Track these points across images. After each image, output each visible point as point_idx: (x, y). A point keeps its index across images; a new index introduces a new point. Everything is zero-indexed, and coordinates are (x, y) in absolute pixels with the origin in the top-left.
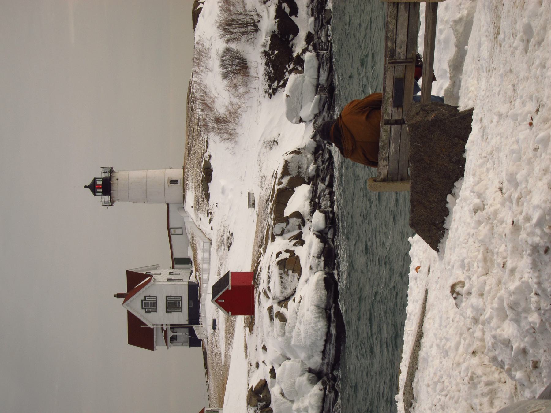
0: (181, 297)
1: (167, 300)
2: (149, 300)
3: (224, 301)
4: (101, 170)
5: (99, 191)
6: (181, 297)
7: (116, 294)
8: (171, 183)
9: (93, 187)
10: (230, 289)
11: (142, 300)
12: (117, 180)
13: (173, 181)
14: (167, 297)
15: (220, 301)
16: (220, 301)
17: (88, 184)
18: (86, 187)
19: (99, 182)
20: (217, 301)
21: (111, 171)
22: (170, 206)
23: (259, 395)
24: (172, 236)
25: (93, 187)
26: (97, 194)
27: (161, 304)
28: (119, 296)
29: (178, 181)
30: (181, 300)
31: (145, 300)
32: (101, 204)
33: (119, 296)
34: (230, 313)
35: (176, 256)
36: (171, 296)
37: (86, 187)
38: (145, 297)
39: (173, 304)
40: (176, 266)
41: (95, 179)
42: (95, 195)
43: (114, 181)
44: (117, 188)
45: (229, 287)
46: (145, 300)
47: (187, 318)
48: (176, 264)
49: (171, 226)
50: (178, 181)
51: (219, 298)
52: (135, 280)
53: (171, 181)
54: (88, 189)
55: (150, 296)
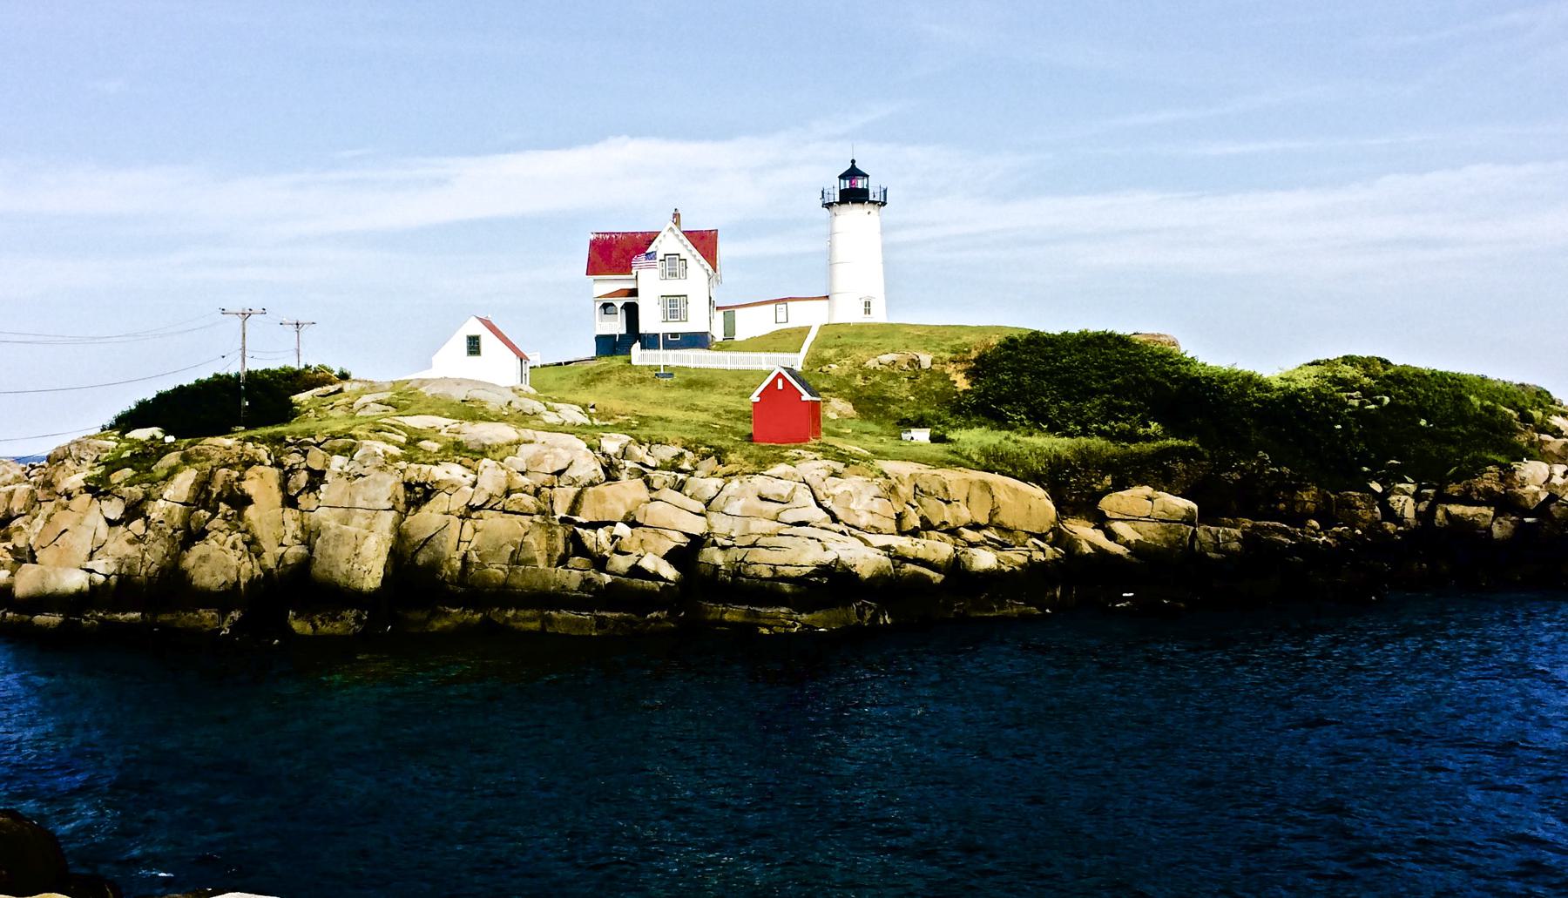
2: (679, 266)
5: (847, 184)
9: (853, 173)
15: (780, 382)
16: (780, 382)
19: (860, 184)
20: (780, 375)
22: (825, 302)
25: (853, 173)
27: (674, 287)
28: (676, 216)
32: (828, 189)
33: (676, 216)
39: (674, 305)
44: (853, 213)
51: (785, 381)
52: (705, 242)
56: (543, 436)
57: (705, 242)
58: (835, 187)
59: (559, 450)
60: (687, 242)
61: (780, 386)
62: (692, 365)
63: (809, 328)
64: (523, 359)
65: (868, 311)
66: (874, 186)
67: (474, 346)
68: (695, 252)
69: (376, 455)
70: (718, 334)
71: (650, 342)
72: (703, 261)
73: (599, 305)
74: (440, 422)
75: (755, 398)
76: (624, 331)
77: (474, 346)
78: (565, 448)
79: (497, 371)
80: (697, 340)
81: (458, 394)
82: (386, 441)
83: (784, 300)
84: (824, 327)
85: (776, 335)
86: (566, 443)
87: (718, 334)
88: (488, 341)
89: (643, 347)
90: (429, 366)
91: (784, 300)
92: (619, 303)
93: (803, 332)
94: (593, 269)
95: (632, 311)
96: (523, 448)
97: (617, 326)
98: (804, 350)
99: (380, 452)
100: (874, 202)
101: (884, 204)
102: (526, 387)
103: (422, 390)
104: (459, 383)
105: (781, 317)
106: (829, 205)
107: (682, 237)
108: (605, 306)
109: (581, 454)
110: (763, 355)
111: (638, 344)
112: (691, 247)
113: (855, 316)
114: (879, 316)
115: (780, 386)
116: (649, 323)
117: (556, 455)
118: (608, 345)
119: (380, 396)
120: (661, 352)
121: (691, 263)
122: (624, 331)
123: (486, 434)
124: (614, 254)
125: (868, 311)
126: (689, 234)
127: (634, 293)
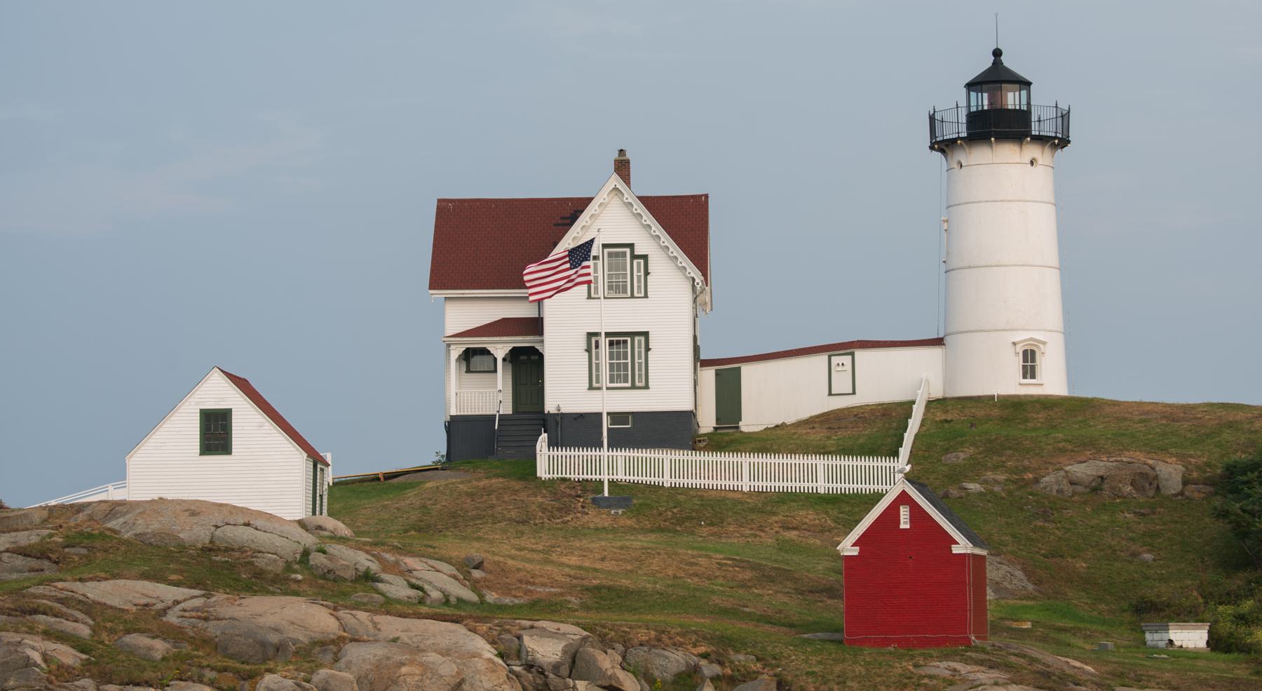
0: (647, 387)
1: (632, 334)
3: (902, 526)
4: (1063, 106)
5: (983, 101)
6: (647, 387)
7: (628, 156)
8: (1025, 352)
9: (997, 77)
10: (956, 550)
11: (631, 246)
12: (1032, 163)
13: (1033, 360)
14: (646, 334)
15: (904, 512)
16: (904, 512)
17: (1006, 61)
18: (997, 53)
19: (1012, 100)
20: (903, 498)
21: (1060, 142)
22: (936, 352)
23: (1257, 673)
24: (823, 358)
25: (997, 77)
26: (973, 95)
27: (619, 315)
29: (1033, 377)
30: (633, 387)
31: (634, 257)
33: (622, 167)
34: (855, 552)
35: (747, 371)
36: (648, 349)
37: (997, 53)
38: (645, 257)
39: (623, 352)
40: (709, 375)
41: (1026, 84)
42: (971, 86)
43: (1032, 151)
45: (962, 546)
46: (634, 257)
47: (564, 410)
48: (718, 373)
49: (860, 354)
50: (1033, 377)
53: (1033, 352)
54: (989, 61)
55: (647, 273)
56: (391, 625)
57: (684, 220)
58: (954, 103)
59: (432, 657)
60: (648, 218)
61: (905, 524)
62: (667, 481)
63: (905, 408)
64: (317, 461)
65: (1029, 371)
66: (1041, 106)
67: (216, 433)
68: (666, 240)
69: (28, 663)
70: (707, 421)
71: (578, 430)
72: (684, 260)
73: (456, 352)
74: (165, 593)
75: (848, 547)
76: (507, 409)
77: (216, 433)
78: (446, 653)
79: (267, 482)
80: (668, 430)
81: (195, 533)
82: (48, 634)
83: (848, 348)
84: (931, 404)
85: (829, 421)
86: (444, 642)
87: (707, 421)
88: (248, 423)
89: (552, 443)
90: (120, 475)
91: (848, 348)
92: (500, 348)
93: (897, 413)
94: (439, 280)
95: (527, 366)
96: (354, 652)
97: (491, 396)
98: (905, 451)
99: (36, 657)
100: (1041, 140)
101: (1064, 142)
102: (331, 523)
103: (113, 524)
104: (194, 509)
105: (842, 382)
106: (943, 146)
107: (639, 208)
108: (468, 355)
109: (480, 665)
110: (821, 463)
111: (544, 436)
112: (657, 229)
113: (1004, 381)
114: (1052, 381)
115: (905, 524)
116: (565, 390)
117: (425, 667)
118: (468, 436)
119: (26, 538)
120: (605, 452)
121: (658, 264)
122: (507, 409)
123: (269, 620)
124: (495, 241)
125: (1029, 371)
126: (649, 203)
127: (535, 326)
